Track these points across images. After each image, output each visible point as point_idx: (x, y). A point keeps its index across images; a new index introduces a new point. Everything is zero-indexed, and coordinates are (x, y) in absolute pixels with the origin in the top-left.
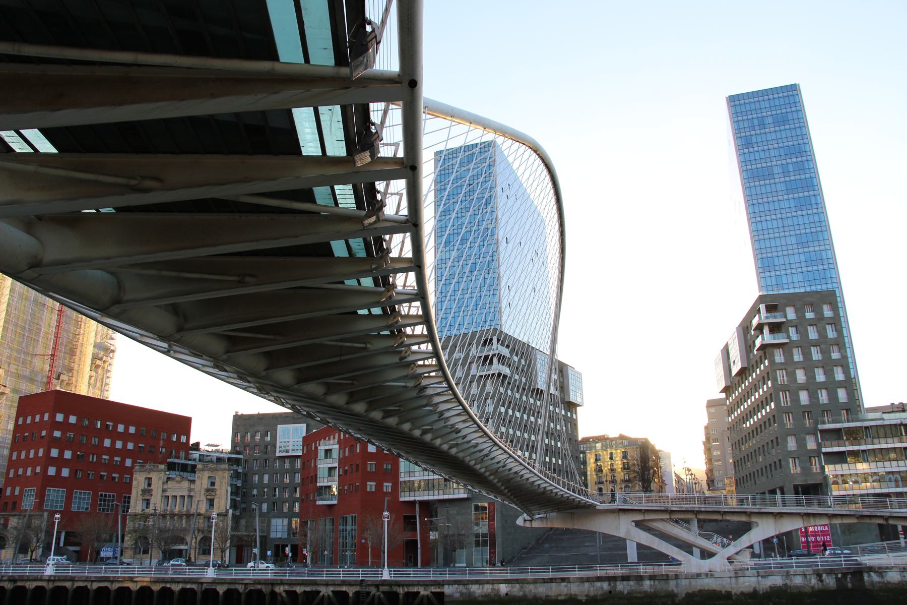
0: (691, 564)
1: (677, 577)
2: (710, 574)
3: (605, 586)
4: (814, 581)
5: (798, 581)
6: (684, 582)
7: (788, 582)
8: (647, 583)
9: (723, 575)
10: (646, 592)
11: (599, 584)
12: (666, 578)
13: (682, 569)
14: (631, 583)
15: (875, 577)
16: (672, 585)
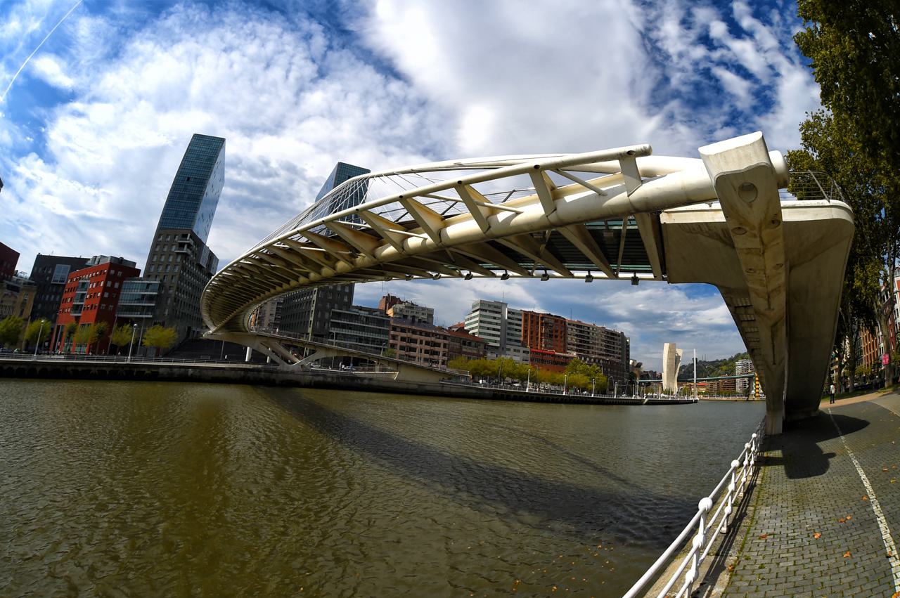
0: (284, 367)
1: (277, 372)
2: (293, 372)
3: (242, 373)
4: (335, 380)
5: (330, 380)
6: (280, 375)
7: (325, 380)
8: (263, 373)
9: (300, 373)
10: (261, 379)
11: (239, 372)
12: (272, 372)
13: (279, 368)
14: (255, 373)
15: (359, 382)
16: (274, 376)
